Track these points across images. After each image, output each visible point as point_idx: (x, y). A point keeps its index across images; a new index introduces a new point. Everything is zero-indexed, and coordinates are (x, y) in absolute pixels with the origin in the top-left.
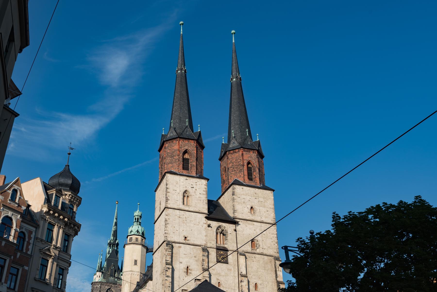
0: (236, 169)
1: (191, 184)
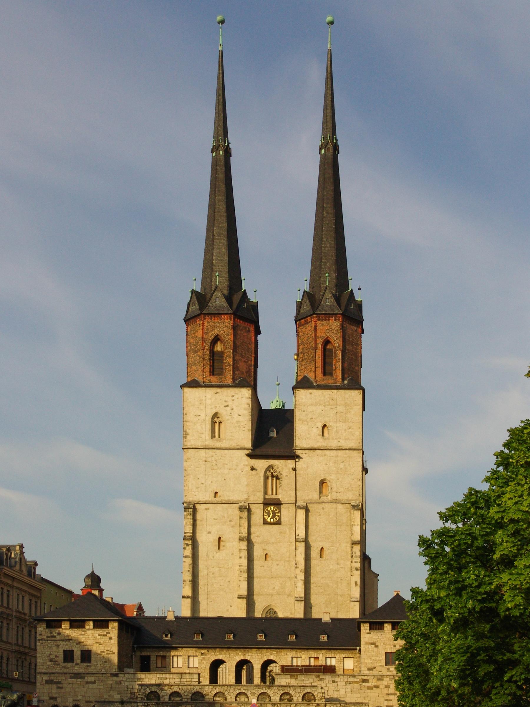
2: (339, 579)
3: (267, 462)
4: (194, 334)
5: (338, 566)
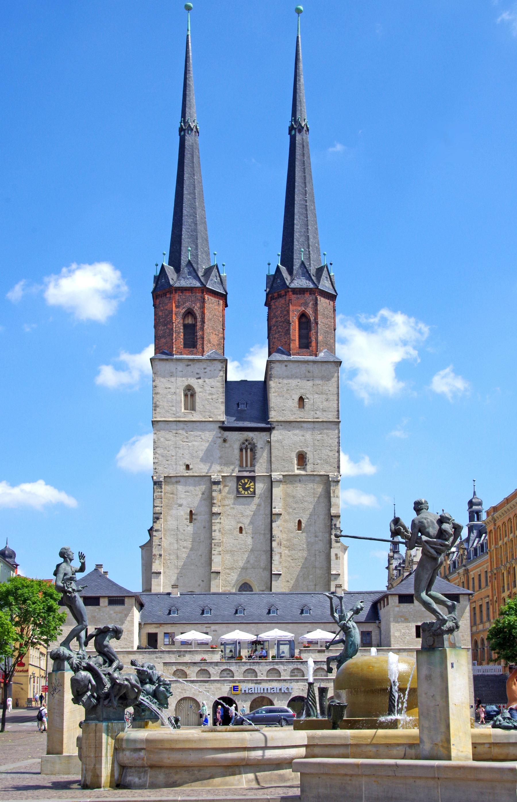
0: (281, 329)
1: (196, 372)
2: (317, 552)
3: (241, 434)
4: (163, 306)
5: (316, 539)
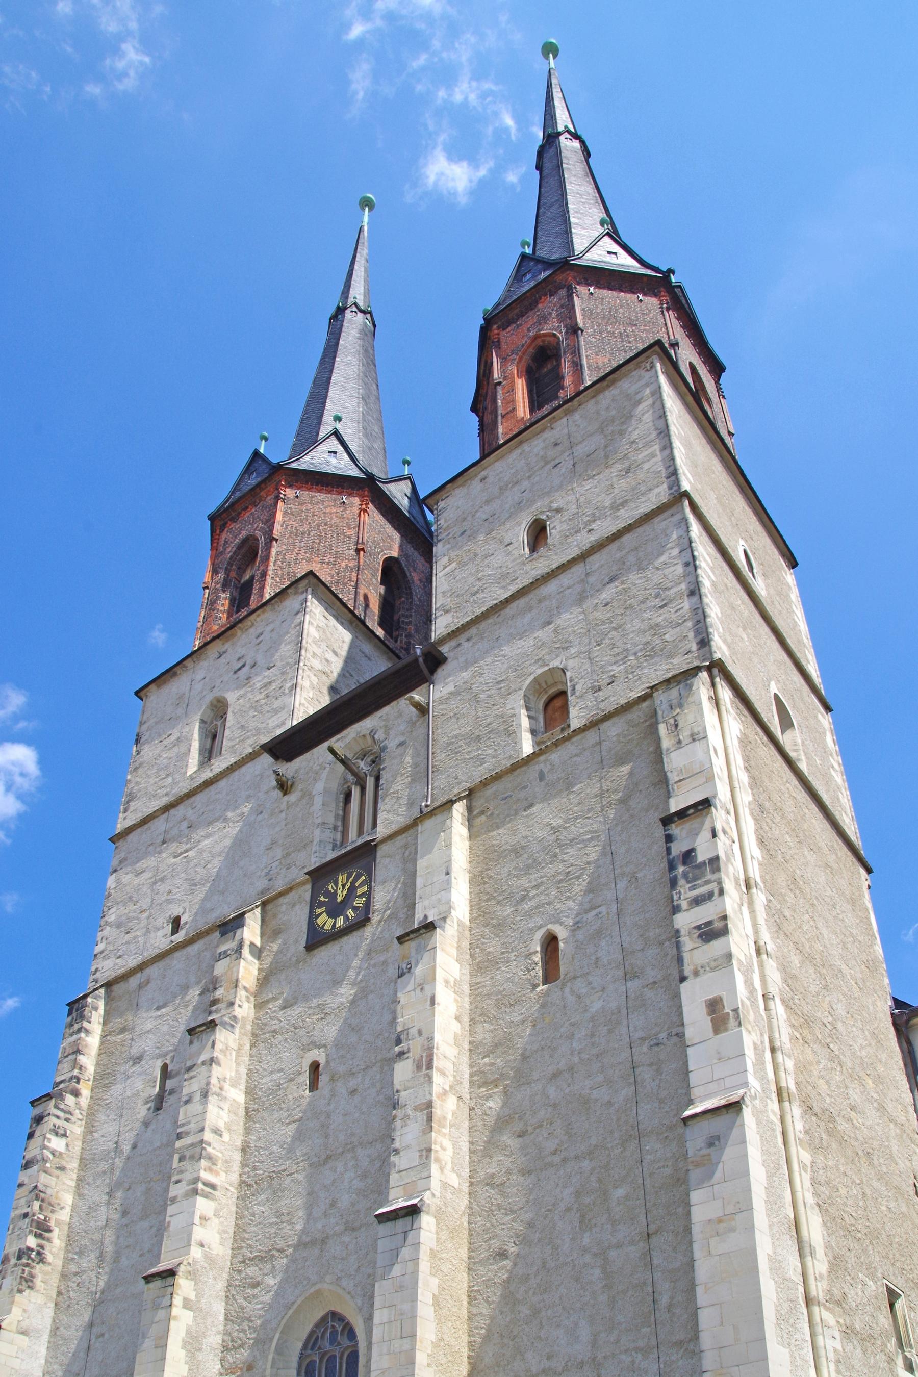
5: (633, 985)
